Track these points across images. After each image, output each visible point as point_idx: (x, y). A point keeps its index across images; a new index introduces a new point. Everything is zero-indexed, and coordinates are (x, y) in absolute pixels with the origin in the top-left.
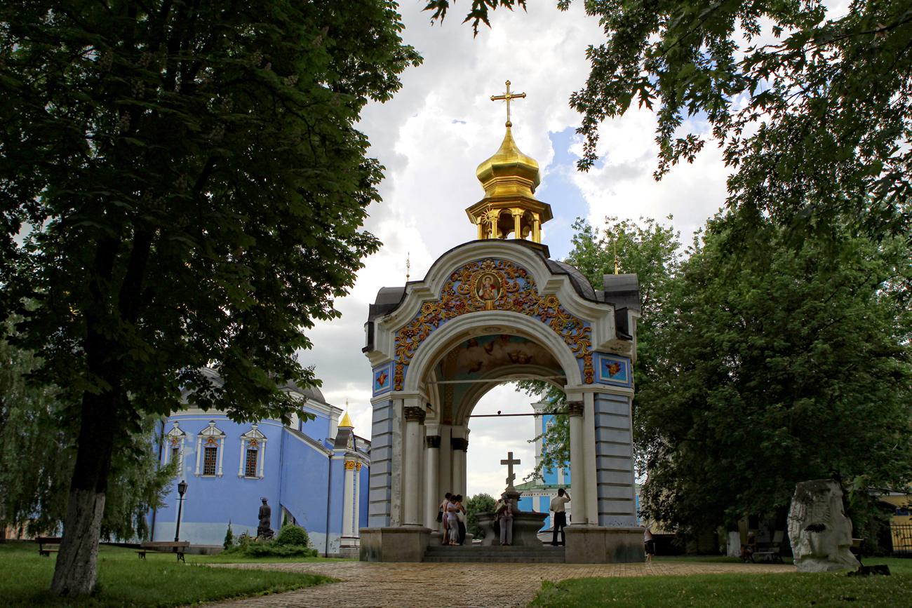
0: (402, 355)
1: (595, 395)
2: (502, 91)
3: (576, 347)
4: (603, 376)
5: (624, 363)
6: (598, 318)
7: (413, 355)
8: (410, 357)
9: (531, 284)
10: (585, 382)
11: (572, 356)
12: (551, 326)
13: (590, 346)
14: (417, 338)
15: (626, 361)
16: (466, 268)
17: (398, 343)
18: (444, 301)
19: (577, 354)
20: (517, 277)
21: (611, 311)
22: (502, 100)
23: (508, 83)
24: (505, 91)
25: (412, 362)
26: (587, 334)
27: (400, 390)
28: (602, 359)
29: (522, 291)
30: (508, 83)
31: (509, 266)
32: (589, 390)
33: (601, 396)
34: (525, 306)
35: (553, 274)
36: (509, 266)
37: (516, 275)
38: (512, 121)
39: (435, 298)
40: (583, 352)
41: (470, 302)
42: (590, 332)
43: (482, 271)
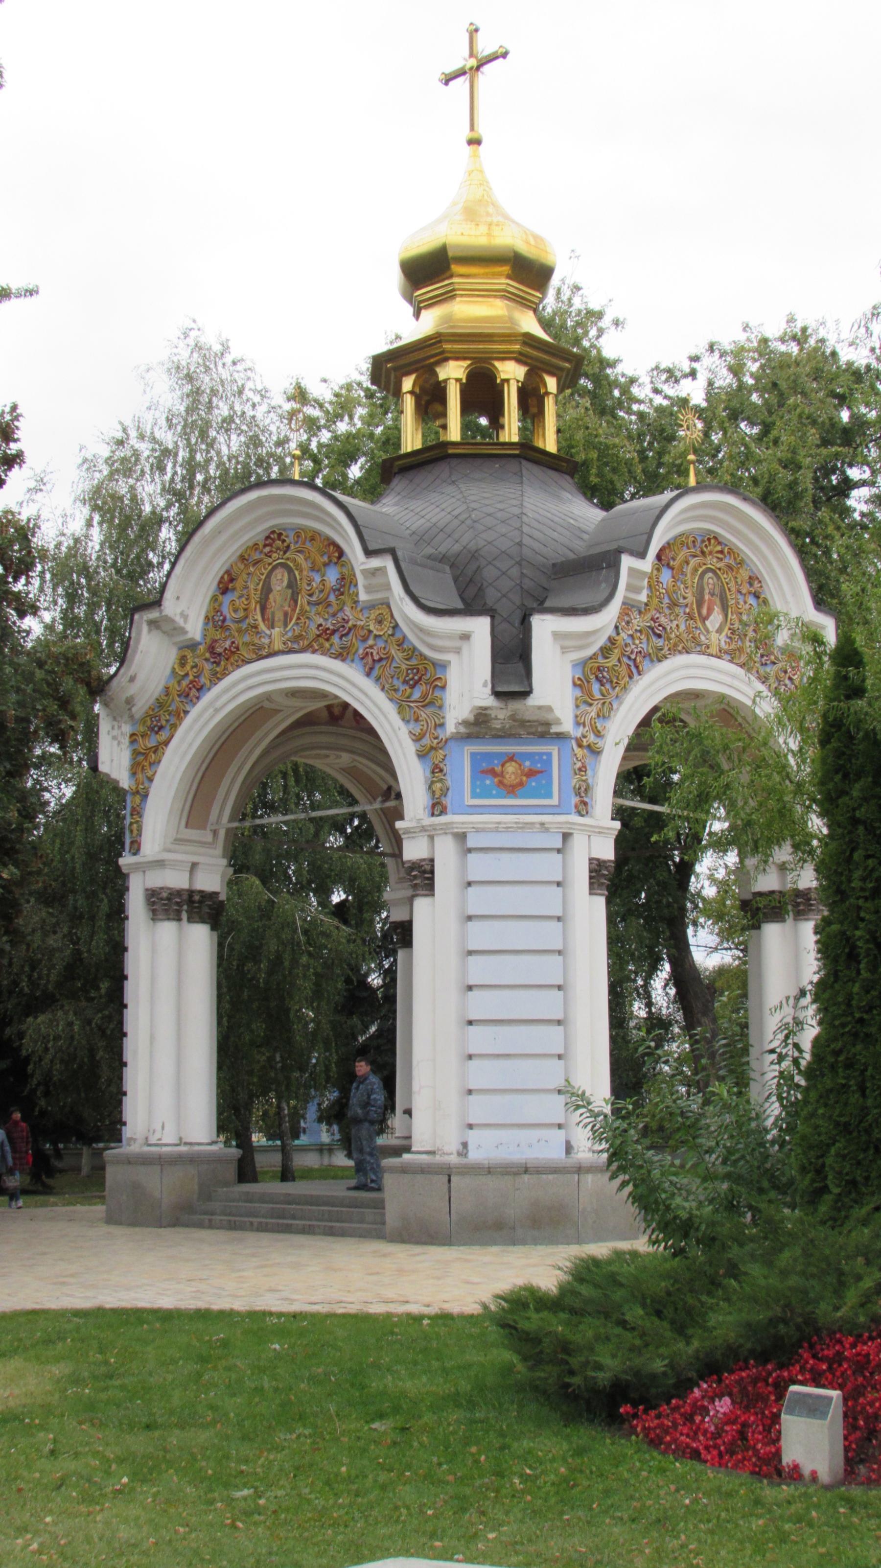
0: (140, 776)
1: (461, 837)
2: (460, 59)
3: (417, 731)
4: (474, 796)
5: (549, 755)
6: (458, 651)
8: (151, 780)
9: (347, 582)
11: (411, 748)
13: (442, 725)
15: (554, 750)
16: (242, 558)
17: (135, 746)
18: (208, 641)
20: (326, 565)
22: (462, 79)
23: (474, 32)
24: (467, 53)
26: (437, 693)
28: (473, 755)
29: (332, 598)
30: (474, 32)
31: (312, 539)
32: (445, 829)
33: (471, 843)
34: (335, 639)
35: (369, 553)
36: (312, 539)
37: (326, 559)
38: (482, 130)
39: (190, 636)
40: (426, 741)
41: (247, 638)
42: (443, 688)
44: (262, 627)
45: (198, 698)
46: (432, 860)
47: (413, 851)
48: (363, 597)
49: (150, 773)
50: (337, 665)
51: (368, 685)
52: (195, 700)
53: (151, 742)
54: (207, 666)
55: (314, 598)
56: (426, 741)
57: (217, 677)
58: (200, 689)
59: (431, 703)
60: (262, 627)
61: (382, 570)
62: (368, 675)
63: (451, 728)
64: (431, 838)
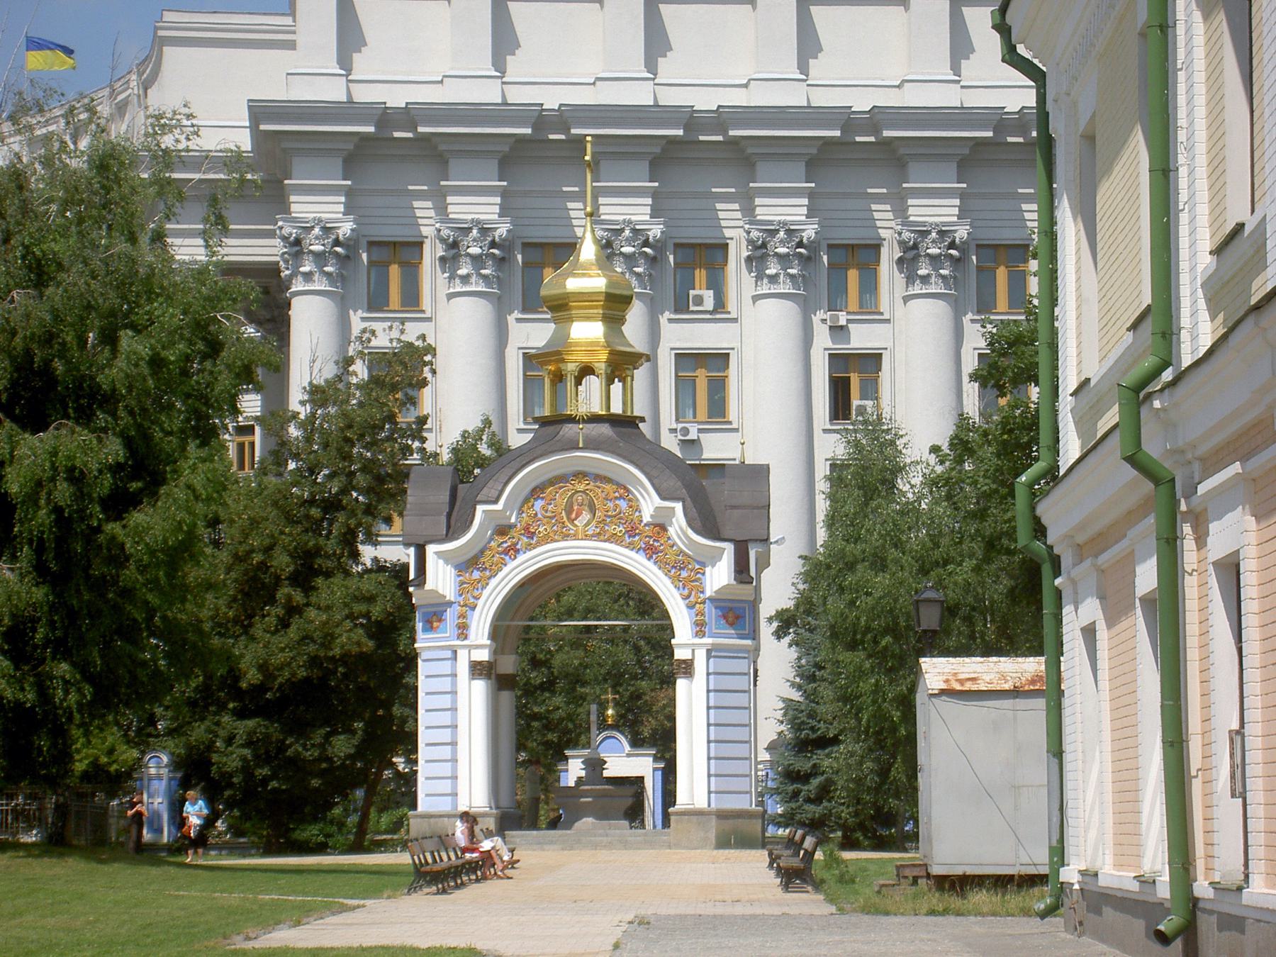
7: (481, 594)
8: (477, 598)
10: (697, 634)
11: (682, 604)
12: (655, 563)
14: (488, 573)
20: (616, 498)
21: (729, 548)
25: (480, 603)
27: (466, 638)
35: (663, 498)
37: (617, 494)
45: (515, 557)
46: (692, 660)
47: (680, 654)
48: (647, 518)
50: (626, 551)
51: (650, 564)
53: (476, 575)
54: (525, 539)
56: (692, 599)
57: (530, 547)
58: (517, 551)
59: (695, 581)
62: (649, 559)
63: (708, 593)
64: (693, 650)
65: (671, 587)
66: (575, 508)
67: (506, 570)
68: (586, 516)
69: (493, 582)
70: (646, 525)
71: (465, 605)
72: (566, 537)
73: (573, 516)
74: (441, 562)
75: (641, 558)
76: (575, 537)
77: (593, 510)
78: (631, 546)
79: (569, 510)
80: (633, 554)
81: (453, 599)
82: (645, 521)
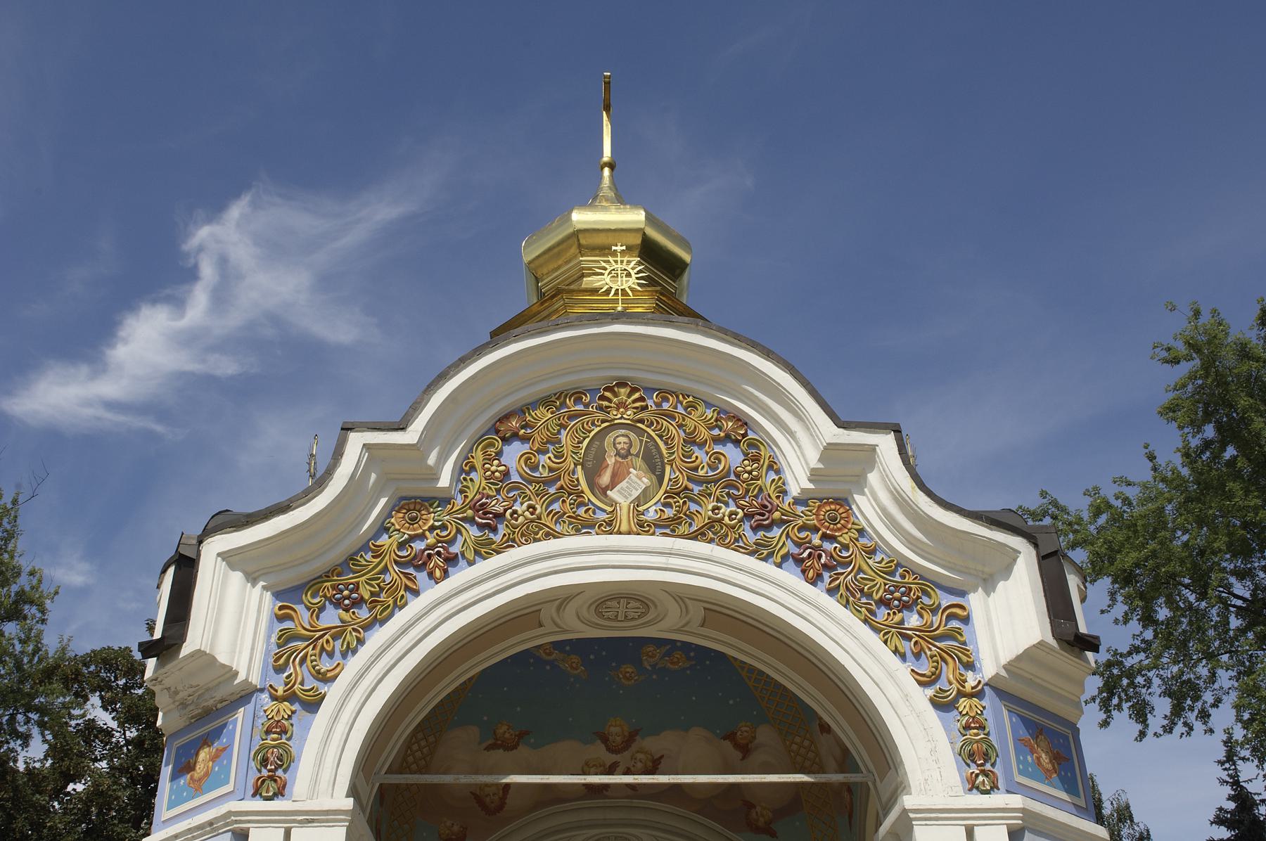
8: (326, 678)
10: (973, 786)
14: (363, 614)
19: (930, 692)
25: (333, 693)
26: (954, 624)
27: (279, 793)
43: (601, 416)
44: (588, 495)
49: (325, 665)
52: (438, 573)
55: (701, 473)
57: (484, 550)
60: (588, 495)
61: (872, 449)
62: (813, 582)
65: (886, 653)
66: (611, 461)
67: (415, 606)
68: (637, 481)
69: (378, 637)
70: (797, 501)
71: (291, 697)
72: (583, 526)
73: (605, 479)
74: (237, 577)
75: (790, 577)
76: (610, 527)
77: (655, 466)
78: (761, 551)
79: (593, 469)
80: (768, 568)
81: (255, 680)
82: (794, 490)
